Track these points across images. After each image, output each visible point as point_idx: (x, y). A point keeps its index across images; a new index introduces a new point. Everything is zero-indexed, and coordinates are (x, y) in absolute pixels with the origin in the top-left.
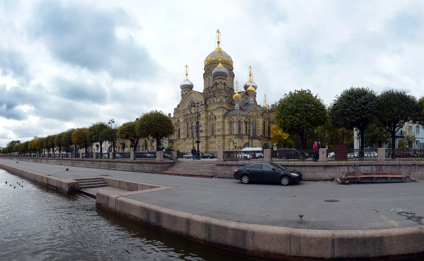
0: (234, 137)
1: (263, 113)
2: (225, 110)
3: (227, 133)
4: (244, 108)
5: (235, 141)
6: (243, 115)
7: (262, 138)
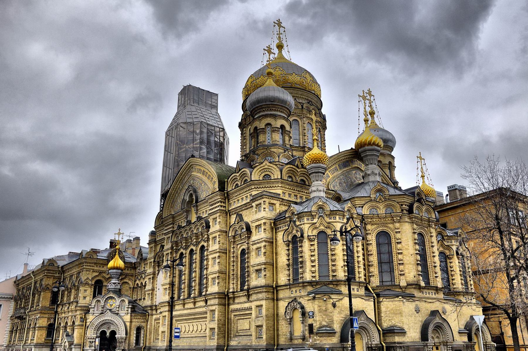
0: (303, 293)
2: (277, 203)
3: (283, 278)
4: (345, 196)
5: (309, 307)
6: (333, 213)
7: (417, 293)
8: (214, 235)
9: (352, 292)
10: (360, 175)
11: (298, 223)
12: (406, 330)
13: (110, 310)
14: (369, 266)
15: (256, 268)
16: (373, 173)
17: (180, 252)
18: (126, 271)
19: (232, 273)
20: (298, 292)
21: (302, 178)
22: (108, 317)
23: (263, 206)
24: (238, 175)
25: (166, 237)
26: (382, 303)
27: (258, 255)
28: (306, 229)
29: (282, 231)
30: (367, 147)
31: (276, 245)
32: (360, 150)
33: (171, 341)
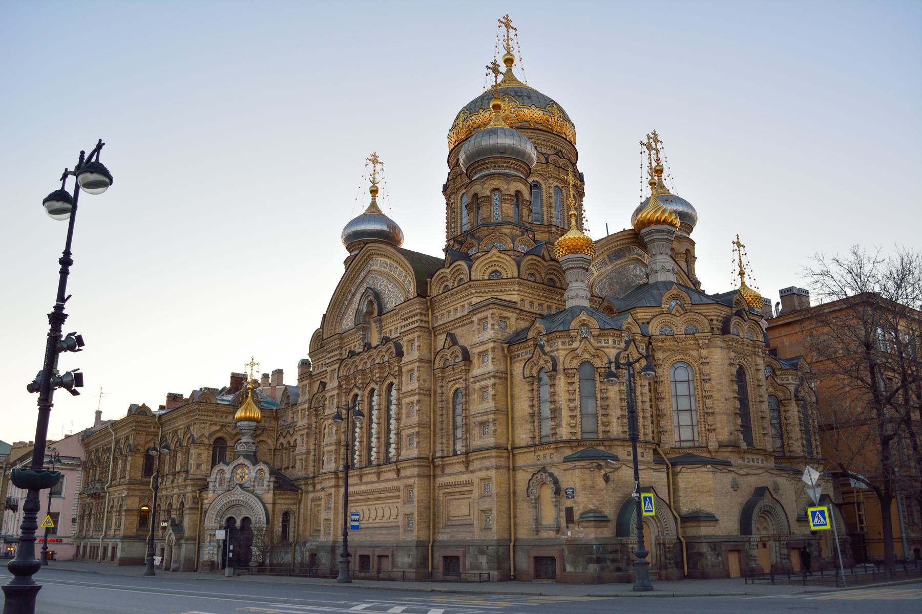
0: (557, 458)
1: (726, 322)
2: (512, 316)
3: (523, 436)
7: (734, 459)
8: (410, 367)
9: (639, 458)
10: (641, 271)
11: (547, 349)
12: (718, 517)
13: (241, 485)
14: (658, 415)
15: (479, 419)
16: (663, 268)
17: (352, 394)
18: (263, 423)
19: (439, 426)
20: (548, 458)
21: (552, 276)
22: (239, 495)
23: (490, 321)
24: (448, 271)
25: (329, 369)
26: (680, 476)
27: (483, 399)
28: (561, 359)
29: (521, 360)
30: (653, 227)
31: (512, 383)
32: (643, 231)
33: (345, 534)
